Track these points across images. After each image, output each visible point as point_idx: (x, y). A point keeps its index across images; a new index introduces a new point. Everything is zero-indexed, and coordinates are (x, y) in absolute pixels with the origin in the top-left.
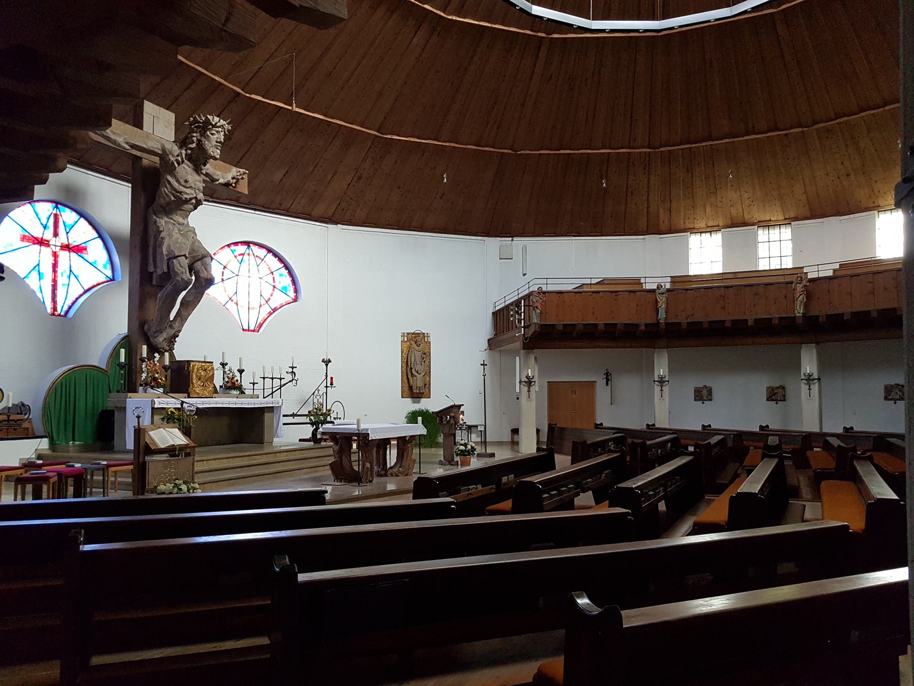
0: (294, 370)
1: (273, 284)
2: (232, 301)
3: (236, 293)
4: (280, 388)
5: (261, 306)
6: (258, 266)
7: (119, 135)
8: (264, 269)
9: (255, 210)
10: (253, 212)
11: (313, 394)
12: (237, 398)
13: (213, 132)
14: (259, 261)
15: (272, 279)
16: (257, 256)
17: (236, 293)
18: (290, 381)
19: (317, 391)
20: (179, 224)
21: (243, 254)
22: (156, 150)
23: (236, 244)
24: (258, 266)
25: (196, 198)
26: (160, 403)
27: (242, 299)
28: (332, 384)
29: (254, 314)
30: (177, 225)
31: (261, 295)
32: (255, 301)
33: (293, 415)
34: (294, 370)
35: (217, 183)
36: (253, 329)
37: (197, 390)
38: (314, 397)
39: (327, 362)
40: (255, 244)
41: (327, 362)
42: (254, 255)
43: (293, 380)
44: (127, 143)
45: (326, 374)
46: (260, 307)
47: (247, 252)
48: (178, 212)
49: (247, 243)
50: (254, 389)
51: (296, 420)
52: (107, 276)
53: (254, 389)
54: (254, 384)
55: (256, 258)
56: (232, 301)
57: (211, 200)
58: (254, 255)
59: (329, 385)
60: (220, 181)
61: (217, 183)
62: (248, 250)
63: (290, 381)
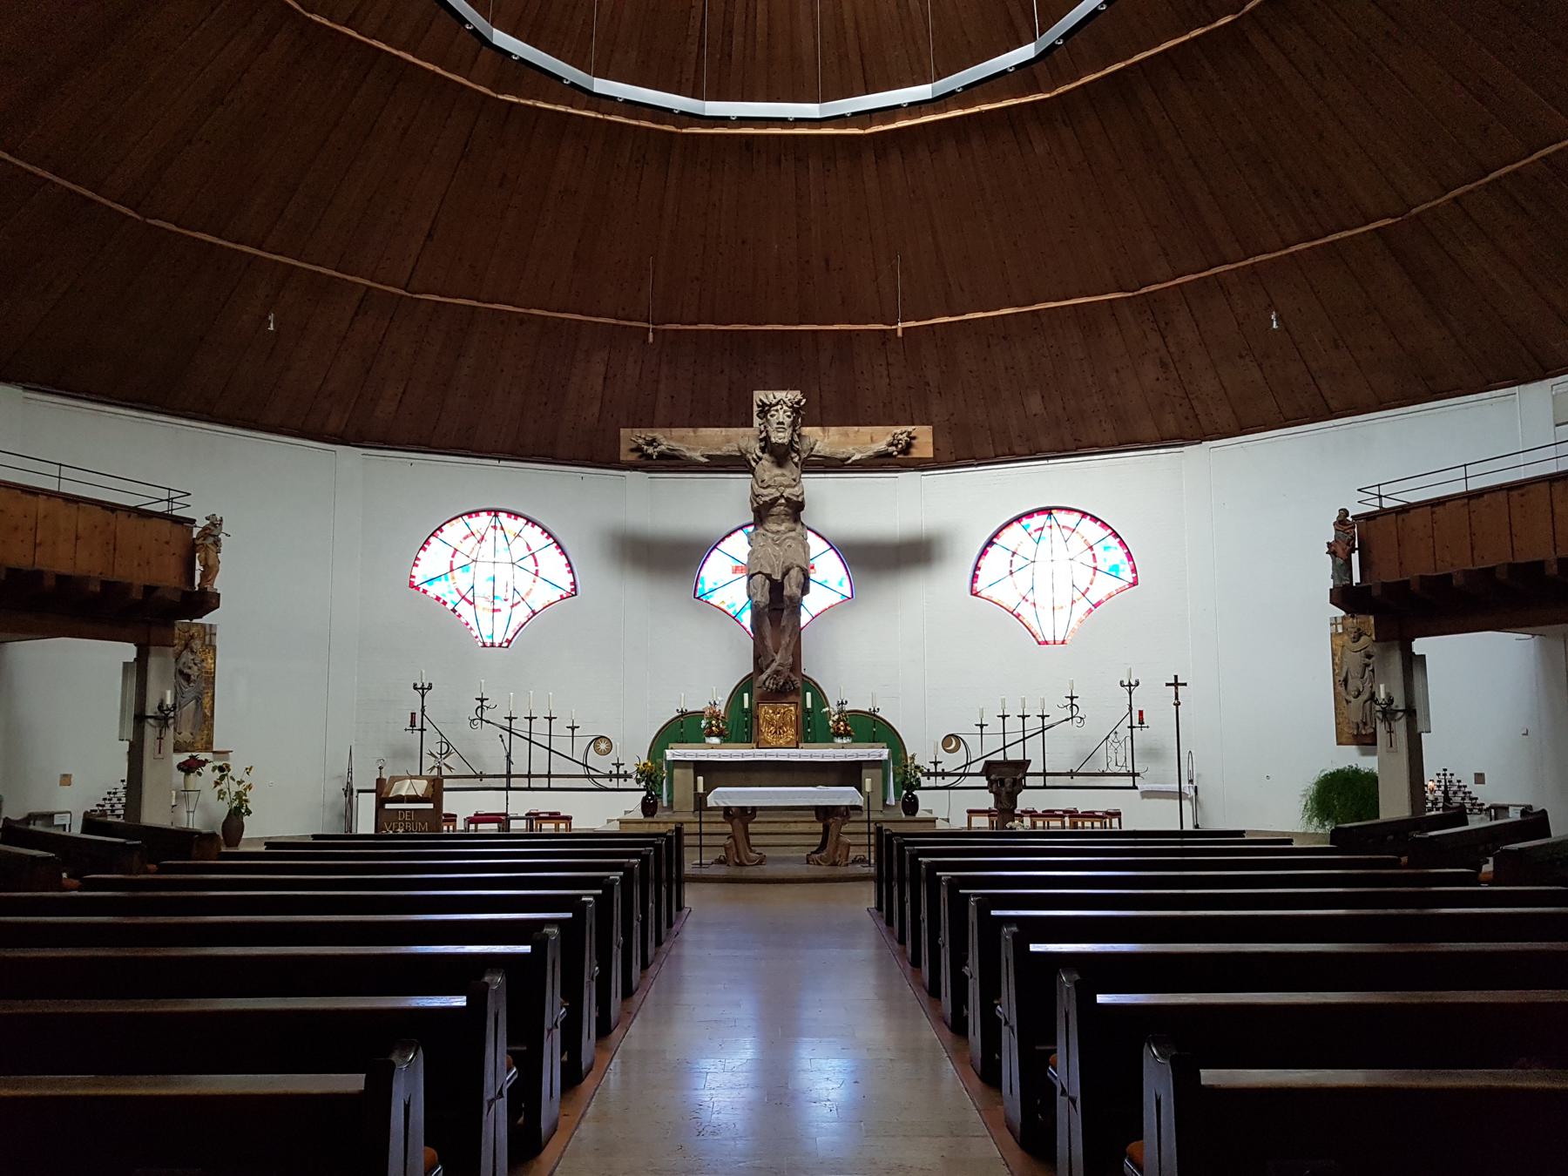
0: (1075, 701)
1: (1093, 565)
2: (1027, 601)
4: (1043, 731)
5: (1073, 602)
6: (1066, 541)
7: (694, 450)
8: (1077, 544)
9: (1047, 458)
10: (1045, 462)
11: (1107, 738)
12: (843, 748)
13: (773, 413)
14: (1067, 533)
15: (1091, 557)
16: (1064, 527)
19: (1112, 735)
20: (773, 533)
21: (1042, 529)
22: (733, 453)
23: (1029, 515)
24: (1066, 541)
25: (782, 496)
26: (673, 755)
27: (1043, 596)
28: (1141, 722)
29: (1062, 616)
30: (769, 535)
31: (1074, 586)
32: (1064, 595)
33: (1071, 774)
35: (850, 461)
36: (1062, 639)
37: (769, 738)
38: (1109, 745)
39: (1130, 687)
40: (1060, 509)
41: (1130, 687)
42: (1059, 525)
44: (702, 456)
45: (1130, 706)
47: (1048, 524)
48: (770, 519)
49: (1047, 511)
50: (982, 734)
51: (1078, 781)
53: (982, 734)
54: (982, 726)
55: (1063, 530)
56: (1027, 601)
57: (976, 463)
58: (1059, 525)
59: (1136, 723)
60: (853, 458)
61: (850, 461)
62: (1049, 520)
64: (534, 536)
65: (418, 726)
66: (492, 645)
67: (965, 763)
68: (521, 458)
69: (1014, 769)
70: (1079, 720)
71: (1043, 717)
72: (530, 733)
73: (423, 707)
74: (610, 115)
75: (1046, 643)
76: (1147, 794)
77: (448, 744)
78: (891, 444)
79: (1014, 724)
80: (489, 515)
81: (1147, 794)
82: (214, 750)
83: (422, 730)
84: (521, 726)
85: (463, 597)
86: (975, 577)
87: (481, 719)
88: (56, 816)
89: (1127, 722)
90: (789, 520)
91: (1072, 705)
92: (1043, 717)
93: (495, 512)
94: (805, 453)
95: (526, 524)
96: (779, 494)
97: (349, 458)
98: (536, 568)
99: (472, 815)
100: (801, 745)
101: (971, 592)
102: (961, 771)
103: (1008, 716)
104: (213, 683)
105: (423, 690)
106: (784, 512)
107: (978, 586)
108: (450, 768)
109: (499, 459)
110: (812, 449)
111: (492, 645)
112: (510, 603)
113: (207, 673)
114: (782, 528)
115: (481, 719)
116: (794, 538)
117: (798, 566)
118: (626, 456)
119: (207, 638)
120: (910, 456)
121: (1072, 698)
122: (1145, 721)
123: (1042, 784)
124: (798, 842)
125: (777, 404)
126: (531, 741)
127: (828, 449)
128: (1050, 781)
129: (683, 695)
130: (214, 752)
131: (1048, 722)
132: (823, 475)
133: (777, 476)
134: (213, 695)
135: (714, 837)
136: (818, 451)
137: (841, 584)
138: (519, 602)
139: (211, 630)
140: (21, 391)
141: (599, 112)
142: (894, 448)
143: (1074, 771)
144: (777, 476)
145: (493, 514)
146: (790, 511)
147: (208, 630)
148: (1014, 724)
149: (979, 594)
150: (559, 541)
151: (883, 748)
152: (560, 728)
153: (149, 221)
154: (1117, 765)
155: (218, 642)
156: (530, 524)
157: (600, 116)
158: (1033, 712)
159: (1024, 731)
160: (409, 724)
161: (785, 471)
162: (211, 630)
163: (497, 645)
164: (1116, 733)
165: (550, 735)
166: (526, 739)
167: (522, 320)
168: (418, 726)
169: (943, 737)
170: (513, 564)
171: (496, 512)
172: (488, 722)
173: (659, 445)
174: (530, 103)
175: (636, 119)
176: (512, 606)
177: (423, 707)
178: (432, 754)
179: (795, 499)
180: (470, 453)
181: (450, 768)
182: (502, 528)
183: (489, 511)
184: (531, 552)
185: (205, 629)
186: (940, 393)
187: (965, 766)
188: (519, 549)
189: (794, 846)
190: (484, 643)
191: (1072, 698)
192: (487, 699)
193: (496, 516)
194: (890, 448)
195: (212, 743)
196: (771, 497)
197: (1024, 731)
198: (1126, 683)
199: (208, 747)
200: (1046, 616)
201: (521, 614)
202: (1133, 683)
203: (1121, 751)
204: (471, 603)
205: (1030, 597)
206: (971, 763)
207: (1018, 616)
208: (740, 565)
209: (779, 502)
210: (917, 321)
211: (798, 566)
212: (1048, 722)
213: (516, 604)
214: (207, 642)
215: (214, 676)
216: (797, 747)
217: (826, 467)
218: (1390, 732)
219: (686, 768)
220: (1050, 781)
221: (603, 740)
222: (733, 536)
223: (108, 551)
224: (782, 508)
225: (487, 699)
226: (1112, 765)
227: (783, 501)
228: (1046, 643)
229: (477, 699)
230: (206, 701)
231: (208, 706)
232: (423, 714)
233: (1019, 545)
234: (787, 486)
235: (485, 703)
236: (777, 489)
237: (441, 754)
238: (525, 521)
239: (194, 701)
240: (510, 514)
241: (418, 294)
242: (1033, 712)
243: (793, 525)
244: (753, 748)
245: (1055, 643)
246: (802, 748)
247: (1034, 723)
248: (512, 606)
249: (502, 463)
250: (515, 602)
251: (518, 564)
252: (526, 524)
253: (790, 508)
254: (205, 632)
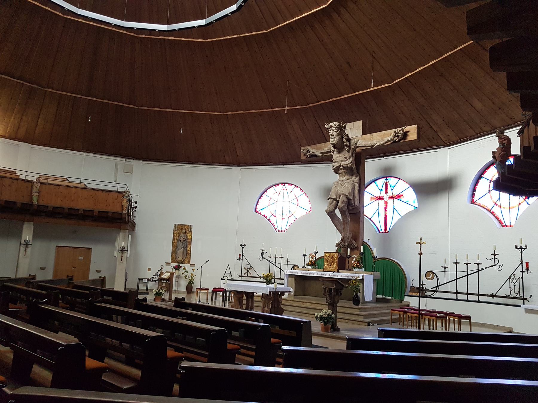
0: (496, 257)
2: (497, 205)
3: (499, 198)
4: (478, 272)
5: (520, 204)
11: (510, 278)
17: (499, 198)
18: (492, 266)
19: (512, 276)
26: (287, 272)
28: (527, 269)
33: (493, 296)
34: (496, 257)
35: (374, 147)
38: (511, 281)
43: (495, 265)
45: (522, 260)
46: (519, 205)
50: (445, 272)
51: (496, 300)
52: (415, 207)
53: (445, 272)
56: (497, 205)
59: (524, 270)
60: (376, 145)
61: (374, 147)
63: (492, 266)
64: (297, 191)
65: (241, 259)
66: (282, 231)
67: (436, 286)
68: (168, 161)
69: (331, 284)
70: (498, 267)
71: (478, 264)
72: (275, 263)
73: (243, 252)
74: (242, 34)
75: (507, 226)
76: (528, 311)
77: (250, 265)
78: (395, 136)
79: (462, 267)
80: (282, 185)
81: (528, 311)
82: (191, 263)
83: (242, 260)
84: (273, 260)
85: (272, 215)
86: (473, 195)
87: (262, 257)
88: (143, 279)
89: (520, 269)
90: (347, 175)
91: (495, 258)
92: (478, 264)
93: (284, 184)
94: (353, 146)
95: (295, 187)
96: (339, 165)
97: (236, 170)
98: (298, 203)
99: (213, 289)
100: (339, 271)
101: (472, 202)
102: (434, 289)
103: (459, 263)
104: (191, 243)
105: (243, 246)
106: (343, 172)
107: (475, 199)
108: (251, 274)
109: (283, 165)
110: (356, 144)
111: (282, 231)
112: (288, 216)
113: (189, 240)
114: (344, 179)
115: (262, 257)
116: (348, 183)
117: (343, 194)
118: (303, 158)
119: (190, 229)
120: (406, 140)
121: (495, 255)
122: (529, 269)
123: (456, 298)
124: (295, 310)
125: (330, 128)
126: (275, 266)
127: (363, 143)
128: (482, 298)
129: (305, 248)
130: (190, 264)
131: (480, 267)
132: (404, 155)
133: (337, 157)
134: (191, 247)
135: (289, 306)
136: (359, 145)
137: (414, 202)
138: (291, 216)
139: (191, 227)
140: (142, 162)
141: (238, 35)
142: (397, 138)
143: (494, 294)
144: (337, 157)
145: (283, 184)
146: (346, 171)
147: (190, 227)
148: (462, 267)
149: (475, 203)
150: (264, 191)
151: (372, 274)
152: (283, 261)
153: (140, 108)
154: (515, 293)
155: (193, 230)
156: (296, 187)
157: (239, 36)
158: (473, 261)
159: (467, 271)
160: (238, 258)
161: (340, 155)
162: (191, 227)
163: (283, 231)
164: (514, 274)
165: (281, 264)
166: (274, 264)
167: (261, 114)
168: (241, 259)
169: (427, 271)
170: (290, 202)
171: (284, 184)
172: (264, 258)
173: (310, 152)
174: (215, 39)
175: (251, 32)
176: (289, 217)
177: (243, 252)
178: (245, 269)
179: (346, 166)
180: (163, 161)
181: (251, 274)
182: (286, 190)
183: (282, 184)
184: (296, 197)
185: (189, 227)
186: (431, 109)
187: (437, 287)
188: (292, 196)
189: (294, 312)
190: (279, 230)
191: (495, 255)
192: (265, 250)
193: (284, 185)
194: (395, 138)
195: (190, 261)
196: (336, 166)
197: (467, 271)
198: (519, 247)
199: (189, 262)
200: (506, 212)
201: (292, 220)
202: (523, 247)
203: (517, 284)
204: (275, 217)
205: (498, 203)
206: (440, 286)
207: (492, 213)
208: (373, 196)
209: (340, 168)
210: (400, 78)
211: (343, 194)
212: (480, 267)
213: (290, 216)
214: (190, 231)
215: (191, 241)
216: (338, 272)
217: (405, 151)
218: (122, 256)
219: (292, 277)
220: (482, 298)
221: (296, 266)
222: (371, 185)
223: (96, 202)
224: (342, 170)
225: (265, 250)
226: (512, 292)
227: (342, 167)
228: (507, 226)
229: (261, 250)
230: (189, 249)
231: (189, 250)
232: (243, 255)
233: (493, 177)
234: (342, 161)
235: (264, 251)
236: (338, 163)
237: (248, 269)
238: (294, 186)
239: (183, 248)
240: (289, 184)
241: (225, 113)
242: (473, 261)
243: (350, 177)
244: (322, 271)
245: (510, 226)
246: (340, 272)
247: (473, 267)
248: (289, 217)
249: (285, 166)
250: (290, 216)
251: (292, 202)
252: (295, 187)
253: (345, 170)
254: (189, 227)
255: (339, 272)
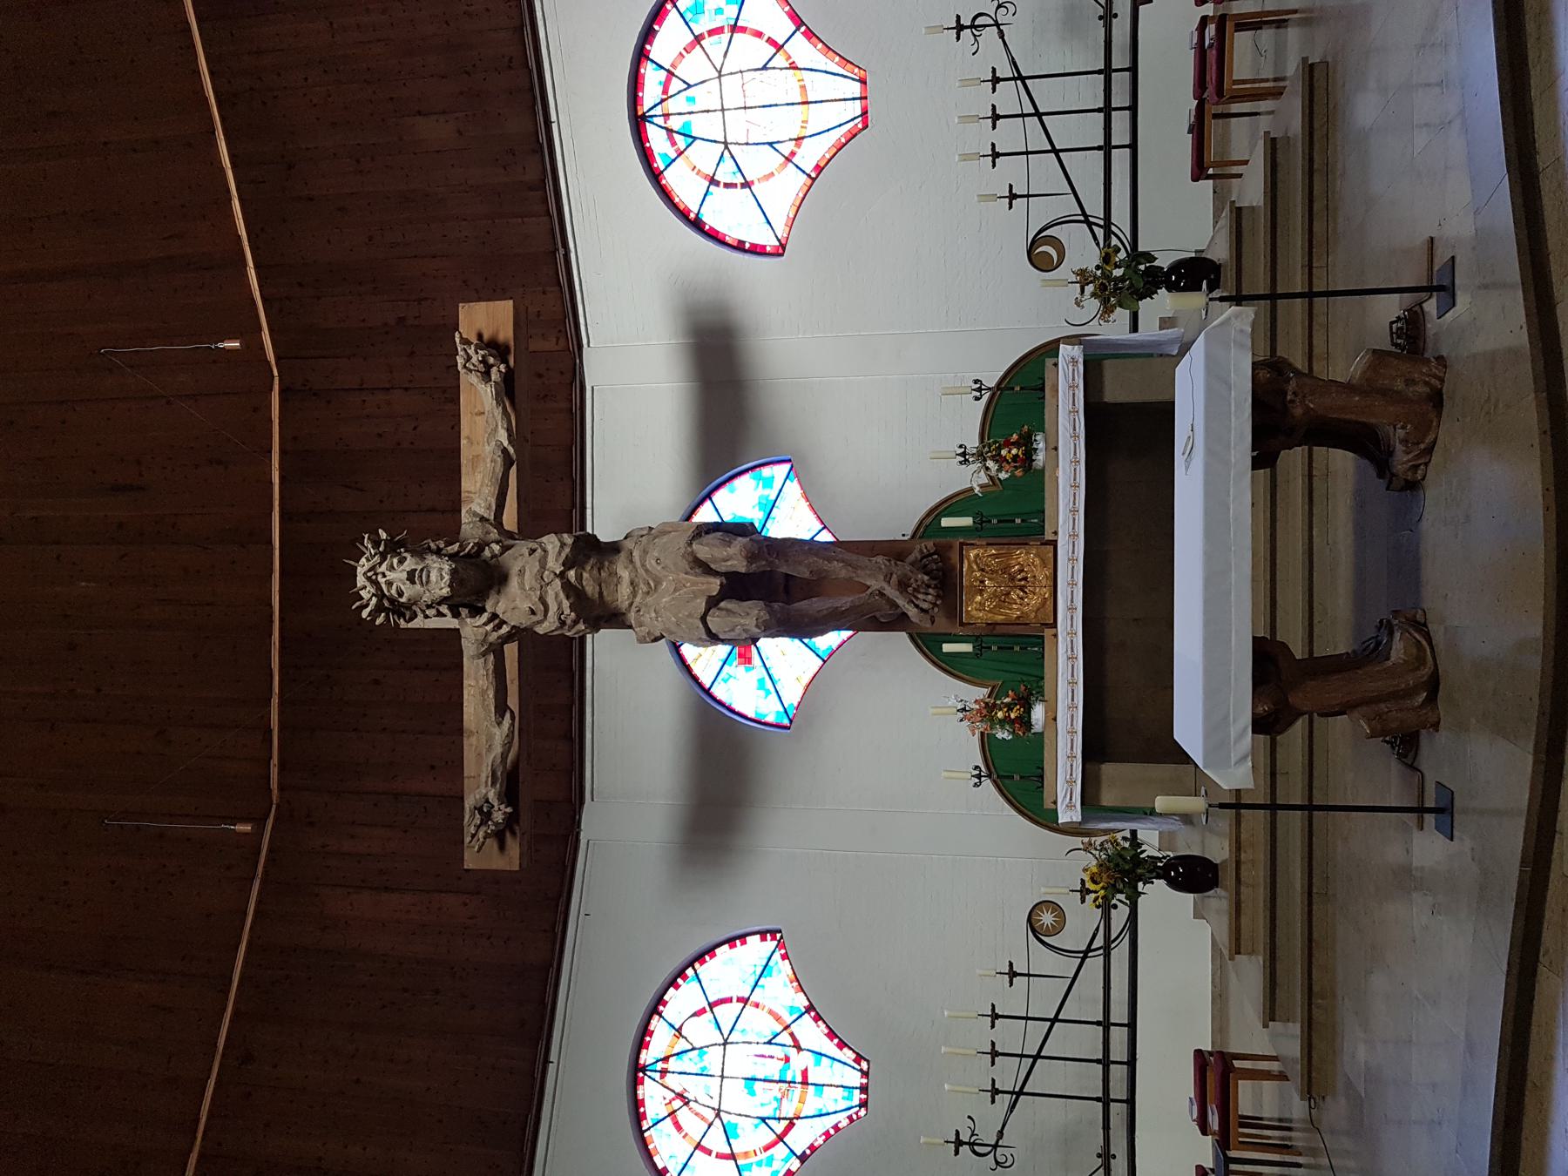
0: (966, 21)
1: (727, 35)
2: (793, 154)
3: (770, 144)
4: (1023, 79)
5: (793, 67)
6: (689, 86)
7: (490, 737)
8: (694, 67)
9: (548, 123)
10: (555, 126)
12: (1056, 449)
13: (393, 592)
14: (676, 85)
15: (715, 38)
16: (665, 91)
17: (770, 144)
18: (1001, 35)
20: (634, 594)
21: (670, 131)
22: (491, 666)
23: (646, 156)
24: (689, 86)
25: (562, 575)
26: (1070, 806)
27: (784, 125)
29: (820, 86)
30: (638, 599)
31: (765, 68)
32: (782, 85)
34: (966, 21)
35: (511, 450)
36: (858, 84)
37: (1034, 601)
40: (634, 99)
42: (663, 101)
43: (997, 25)
44: (499, 724)
46: (796, 68)
47: (660, 121)
48: (608, 598)
49: (639, 123)
50: (1028, 196)
52: (787, 477)
53: (1028, 196)
54: (1013, 196)
55: (671, 93)
56: (793, 154)
57: (562, 251)
58: (663, 101)
60: (506, 443)
61: (511, 450)
62: (655, 120)
63: (1001, 35)
64: (681, 1001)
66: (864, 1089)
72: (1022, 1056)
75: (864, 113)
78: (486, 376)
84: (1008, 1074)
86: (758, 250)
87: (995, 1146)
91: (972, 26)
92: (996, 80)
93: (637, 1071)
94: (488, 533)
96: (558, 582)
100: (1048, 536)
102: (1100, 232)
106: (595, 572)
107: (770, 242)
109: (546, 1061)
110: (483, 519)
112: (792, 1052)
114: (625, 574)
115: (995, 1146)
116: (645, 552)
117: (690, 544)
125: (376, 583)
126: (1037, 1057)
128: (1120, 59)
129: (946, 774)
131: (1005, 71)
132: (589, 512)
136: (489, 508)
138: (792, 1035)
142: (494, 370)
144: (522, 585)
146: (592, 561)
148: (1009, 135)
152: (1012, 1002)
158: (983, 100)
159: (1023, 115)
161: (514, 571)
170: (725, 1043)
172: (1001, 1134)
173: (487, 801)
176: (799, 1048)
179: (567, 550)
183: (636, 1082)
184: (708, 1009)
186: (420, 301)
187: (1090, 225)
188: (701, 1031)
190: (860, 1106)
191: (960, 28)
196: (562, 595)
197: (1023, 115)
201: (811, 1033)
204: (791, 1126)
205: (786, 149)
209: (573, 580)
211: (690, 544)
212: (1005, 71)
216: (1054, 544)
217: (574, 505)
220: (1120, 59)
221: (1035, 917)
224: (585, 575)
227: (572, 574)
234: (543, 563)
235: (965, 1137)
238: (656, 1017)
242: (983, 100)
243: (623, 555)
246: (1056, 533)
247: (1008, 98)
248: (799, 1048)
249: (553, 1057)
252: (660, 1014)
253: (586, 562)
255: (1053, 806)
